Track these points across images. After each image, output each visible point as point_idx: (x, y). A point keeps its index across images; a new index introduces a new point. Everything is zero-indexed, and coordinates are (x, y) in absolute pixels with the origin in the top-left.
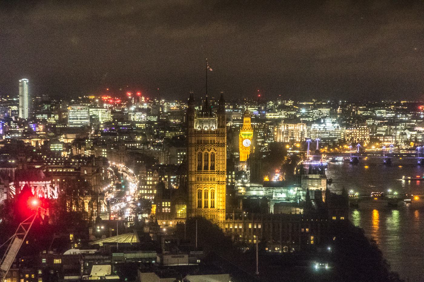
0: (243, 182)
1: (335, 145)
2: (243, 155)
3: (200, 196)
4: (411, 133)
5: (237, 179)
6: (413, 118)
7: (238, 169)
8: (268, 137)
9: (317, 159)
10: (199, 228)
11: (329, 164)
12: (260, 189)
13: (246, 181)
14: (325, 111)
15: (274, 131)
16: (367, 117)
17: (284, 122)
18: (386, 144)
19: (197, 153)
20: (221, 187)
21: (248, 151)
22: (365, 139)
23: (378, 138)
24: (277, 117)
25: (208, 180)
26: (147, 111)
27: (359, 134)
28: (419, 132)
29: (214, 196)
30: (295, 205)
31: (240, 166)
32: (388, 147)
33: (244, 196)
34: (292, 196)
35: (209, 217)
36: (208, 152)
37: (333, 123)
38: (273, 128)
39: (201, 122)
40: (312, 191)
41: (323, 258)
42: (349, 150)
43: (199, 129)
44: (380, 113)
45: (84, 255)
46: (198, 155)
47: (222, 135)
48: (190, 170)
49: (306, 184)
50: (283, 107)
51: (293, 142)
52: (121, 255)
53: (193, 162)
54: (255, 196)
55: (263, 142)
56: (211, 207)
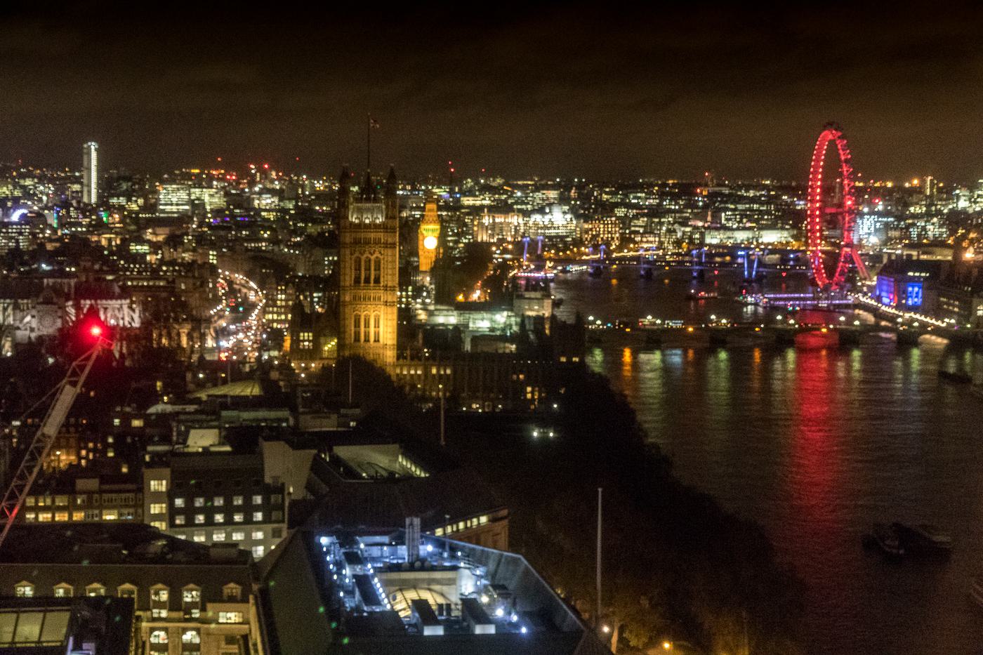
1: (566, 247)
2: (425, 263)
3: (357, 324)
4: (683, 229)
5: (414, 297)
6: (686, 206)
7: (416, 282)
8: (463, 234)
9: (540, 268)
11: (556, 275)
12: (450, 313)
13: (428, 301)
14: (553, 194)
15: (473, 225)
16: (617, 205)
17: (489, 211)
18: (645, 246)
19: (354, 257)
20: (389, 309)
21: (433, 256)
22: (613, 238)
23: (633, 236)
24: (478, 203)
25: (369, 299)
27: (604, 231)
28: (696, 228)
29: (380, 328)
30: (503, 338)
31: (419, 278)
32: (647, 250)
33: (425, 324)
34: (499, 324)
35: (371, 356)
36: (369, 256)
37: (564, 213)
38: (472, 221)
39: (360, 211)
40: (529, 317)
41: (544, 420)
42: (588, 255)
43: (357, 221)
44: (635, 198)
45: (178, 413)
46: (355, 262)
47: (393, 230)
48: (342, 284)
49: (519, 306)
52: (234, 413)
53: (348, 271)
54: (443, 325)
55: (456, 242)
56: (375, 341)
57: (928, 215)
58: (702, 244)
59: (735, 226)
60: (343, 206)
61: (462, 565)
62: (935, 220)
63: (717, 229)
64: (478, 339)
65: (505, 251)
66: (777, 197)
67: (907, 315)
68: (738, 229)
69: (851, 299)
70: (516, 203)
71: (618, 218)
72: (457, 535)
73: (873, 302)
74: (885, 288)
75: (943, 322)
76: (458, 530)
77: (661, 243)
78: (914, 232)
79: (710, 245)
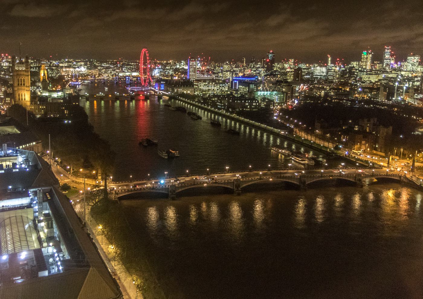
0: (39, 90)
1: (85, 76)
3: (19, 96)
6: (115, 67)
9: (77, 81)
10: (17, 109)
13: (40, 90)
14: (83, 63)
18: (104, 76)
20: (28, 92)
22: (97, 74)
24: (64, 65)
25: (22, 89)
26: (9, 62)
28: (117, 72)
29: (26, 96)
30: (60, 99)
39: (18, 66)
41: (67, 119)
43: (18, 69)
47: (28, 72)
50: (68, 62)
51: (68, 75)
57: (170, 69)
58: (118, 76)
59: (126, 71)
60: (14, 65)
61: (18, 155)
62: (171, 70)
63: (122, 72)
64: (54, 99)
65: (69, 77)
66: (138, 65)
67: (161, 92)
68: (127, 72)
69: (149, 88)
70: (74, 65)
71: (98, 69)
72: (26, 148)
73: (154, 89)
74: (157, 86)
75: (168, 93)
76: (27, 146)
77: (108, 75)
78: (167, 73)
79: (120, 76)
